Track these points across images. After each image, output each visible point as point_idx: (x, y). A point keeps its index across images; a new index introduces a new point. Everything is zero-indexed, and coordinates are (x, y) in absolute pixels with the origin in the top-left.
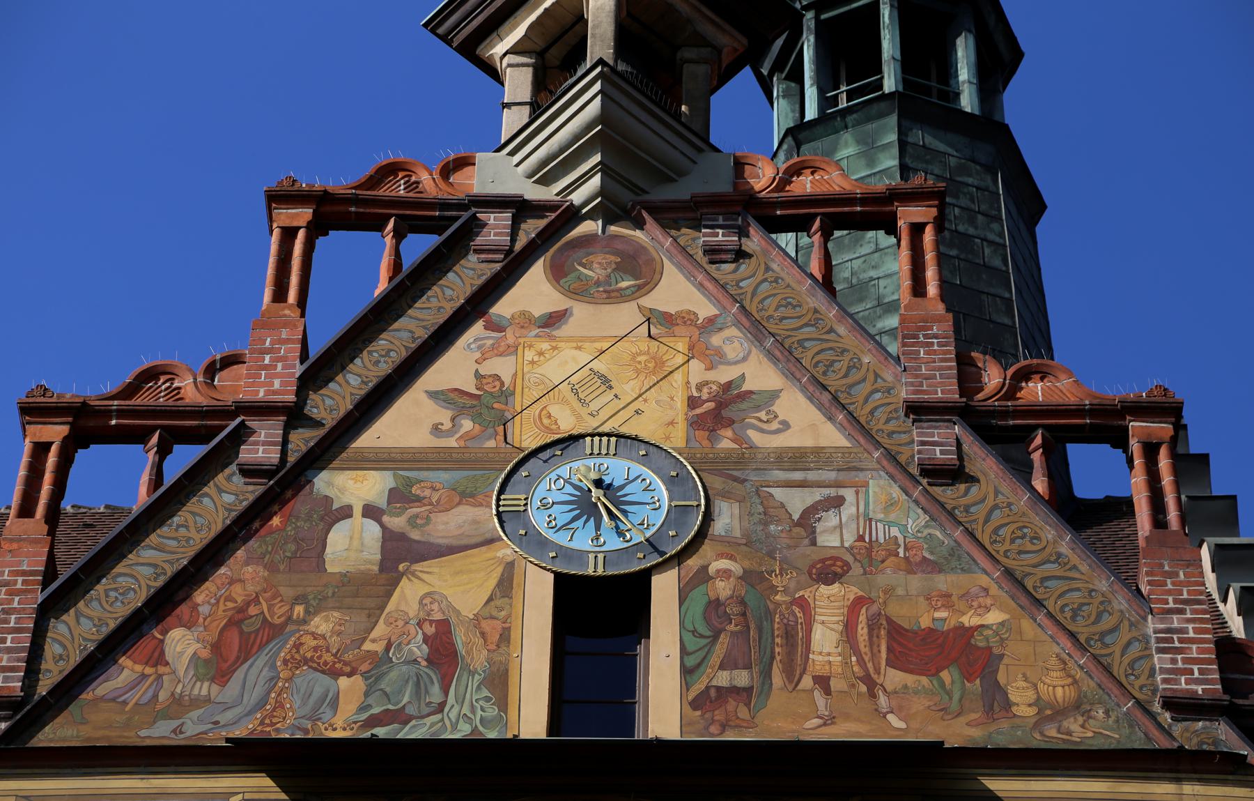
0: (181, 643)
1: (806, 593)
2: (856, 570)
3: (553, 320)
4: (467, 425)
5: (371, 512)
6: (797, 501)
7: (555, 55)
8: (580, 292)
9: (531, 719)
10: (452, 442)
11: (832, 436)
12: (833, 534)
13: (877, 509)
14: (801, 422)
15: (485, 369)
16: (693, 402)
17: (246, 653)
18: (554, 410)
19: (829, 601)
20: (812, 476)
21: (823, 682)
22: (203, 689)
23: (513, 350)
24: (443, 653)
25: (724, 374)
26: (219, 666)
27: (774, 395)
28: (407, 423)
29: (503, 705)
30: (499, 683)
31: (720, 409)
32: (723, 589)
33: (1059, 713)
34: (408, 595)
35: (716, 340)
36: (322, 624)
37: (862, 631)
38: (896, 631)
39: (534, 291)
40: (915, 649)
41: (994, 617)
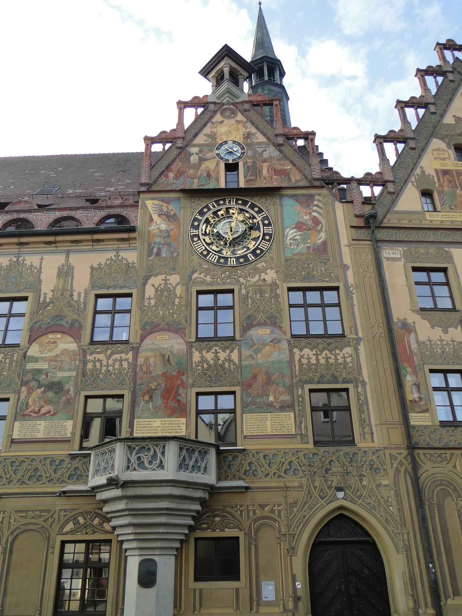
0: (171, 175)
1: (262, 165)
2: (269, 161)
3: (222, 122)
4: (210, 139)
5: (196, 154)
6: (260, 150)
7: (219, 77)
8: (225, 118)
9: (223, 186)
10: (208, 142)
11: (265, 140)
12: (266, 155)
13: (271, 152)
14: (260, 138)
15: (212, 130)
16: (244, 135)
17: (180, 176)
18: (223, 137)
19: (265, 166)
20: (262, 146)
21: (265, 178)
22: (175, 181)
23: (216, 127)
24: (209, 175)
25: (248, 130)
26: (177, 178)
27: (256, 133)
28: (201, 139)
29: (218, 183)
30: (217, 180)
31: (248, 136)
32: (249, 164)
33: (299, 181)
34: (203, 166)
35: (247, 125)
36: (191, 171)
37: (270, 170)
38: (275, 170)
39: (218, 117)
40: (278, 172)
41: (289, 167)
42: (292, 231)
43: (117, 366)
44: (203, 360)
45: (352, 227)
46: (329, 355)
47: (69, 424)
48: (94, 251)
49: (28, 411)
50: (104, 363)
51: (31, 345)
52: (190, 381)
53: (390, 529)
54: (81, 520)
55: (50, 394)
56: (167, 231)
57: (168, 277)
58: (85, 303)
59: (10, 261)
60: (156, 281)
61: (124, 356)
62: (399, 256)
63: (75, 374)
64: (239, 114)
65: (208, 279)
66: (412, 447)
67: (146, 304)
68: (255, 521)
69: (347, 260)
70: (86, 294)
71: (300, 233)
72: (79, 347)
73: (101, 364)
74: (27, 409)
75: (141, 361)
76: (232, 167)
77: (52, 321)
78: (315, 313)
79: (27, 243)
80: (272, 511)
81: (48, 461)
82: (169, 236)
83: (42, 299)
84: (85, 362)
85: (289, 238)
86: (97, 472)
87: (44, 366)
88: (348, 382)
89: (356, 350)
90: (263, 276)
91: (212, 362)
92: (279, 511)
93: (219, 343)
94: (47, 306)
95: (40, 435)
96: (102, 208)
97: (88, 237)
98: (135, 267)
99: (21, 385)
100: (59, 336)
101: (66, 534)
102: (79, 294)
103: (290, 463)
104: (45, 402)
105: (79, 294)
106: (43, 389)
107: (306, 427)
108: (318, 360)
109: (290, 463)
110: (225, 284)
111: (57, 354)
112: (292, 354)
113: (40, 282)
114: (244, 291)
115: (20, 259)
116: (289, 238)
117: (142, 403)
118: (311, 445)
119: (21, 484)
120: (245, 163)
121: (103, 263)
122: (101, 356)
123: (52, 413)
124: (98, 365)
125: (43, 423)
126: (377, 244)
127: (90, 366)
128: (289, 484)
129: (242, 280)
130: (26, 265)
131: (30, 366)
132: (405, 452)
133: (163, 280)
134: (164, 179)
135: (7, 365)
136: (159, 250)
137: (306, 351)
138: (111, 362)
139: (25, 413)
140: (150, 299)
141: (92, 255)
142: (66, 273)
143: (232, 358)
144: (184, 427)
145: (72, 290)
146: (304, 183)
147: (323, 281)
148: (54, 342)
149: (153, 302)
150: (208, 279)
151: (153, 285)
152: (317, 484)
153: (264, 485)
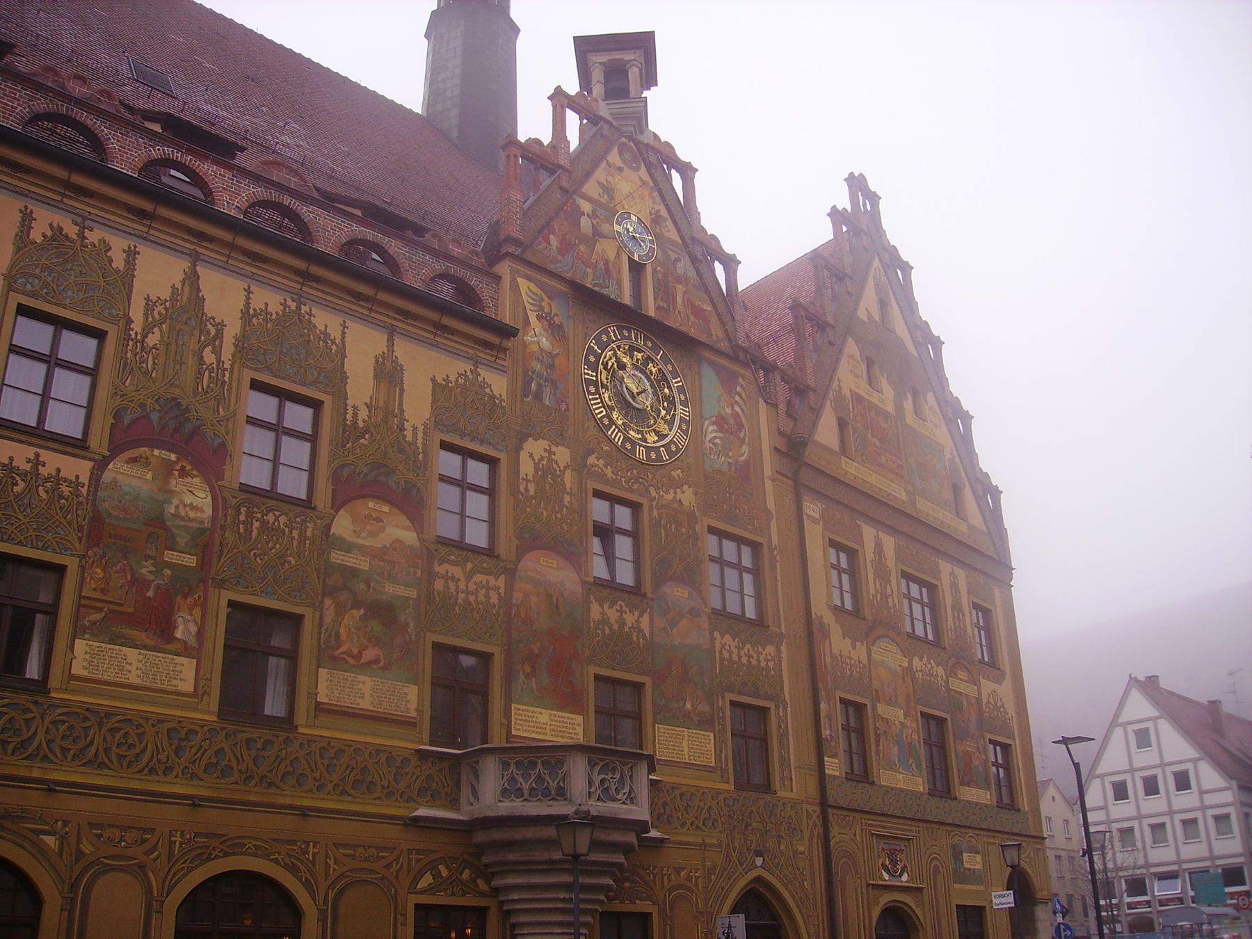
3: (621, 169)
6: (674, 256)
25: (657, 208)
31: (656, 219)
41: (709, 308)
42: (711, 428)
43: (481, 598)
44: (604, 621)
45: (776, 449)
46: (752, 652)
47: (412, 692)
48: (435, 346)
49: (341, 650)
50: (462, 586)
51: (337, 511)
52: (587, 653)
53: (804, 910)
54: (444, 873)
55: (376, 626)
56: (553, 356)
57: (553, 448)
58: (425, 453)
59: (284, 305)
60: (535, 448)
61: (492, 579)
62: (817, 516)
63: (414, 594)
64: (643, 168)
65: (609, 471)
66: (824, 804)
67: (522, 489)
68: (671, 890)
69: (771, 504)
70: (425, 433)
71: (720, 435)
72: (421, 540)
73: (457, 587)
74: (339, 647)
75: (517, 597)
76: (636, 268)
77: (372, 471)
78: (731, 576)
79: (317, 280)
80: (689, 879)
81: (383, 757)
82: (553, 366)
83: (349, 417)
84: (431, 576)
85: (709, 437)
86: (505, 793)
87: (364, 565)
88: (770, 698)
89: (779, 651)
90: (679, 495)
91: (615, 627)
92: (697, 878)
93: (626, 596)
94: (359, 437)
95: (365, 704)
96: (435, 253)
97: (434, 316)
98: (503, 408)
99: (324, 595)
100: (386, 509)
101: (422, 892)
102: (415, 429)
103: (710, 809)
104: (369, 641)
105: (415, 429)
106: (362, 612)
107: (726, 759)
108: (740, 657)
109: (710, 809)
110: (630, 490)
111: (385, 547)
112: (713, 639)
113: (344, 378)
114: (655, 513)
115: (304, 309)
116: (709, 437)
117: (522, 678)
118: (731, 787)
119: (341, 794)
120: (654, 271)
121: (452, 378)
122: (456, 571)
123: (382, 664)
124: (452, 585)
125: (367, 679)
126: (798, 490)
127: (439, 584)
128: (707, 841)
129: (652, 490)
130: (315, 327)
131: (337, 557)
132: (817, 808)
133: (546, 450)
134: (544, 245)
135: (295, 543)
136: (540, 386)
137: (728, 639)
138: (472, 587)
139: (336, 653)
140: (527, 481)
141: (433, 354)
142: (388, 374)
143: (642, 626)
144: (580, 730)
145: (403, 420)
146: (724, 346)
147: (746, 529)
148: (378, 520)
149: (532, 489)
150: (609, 471)
151: (531, 455)
152: (736, 844)
153: (684, 839)
